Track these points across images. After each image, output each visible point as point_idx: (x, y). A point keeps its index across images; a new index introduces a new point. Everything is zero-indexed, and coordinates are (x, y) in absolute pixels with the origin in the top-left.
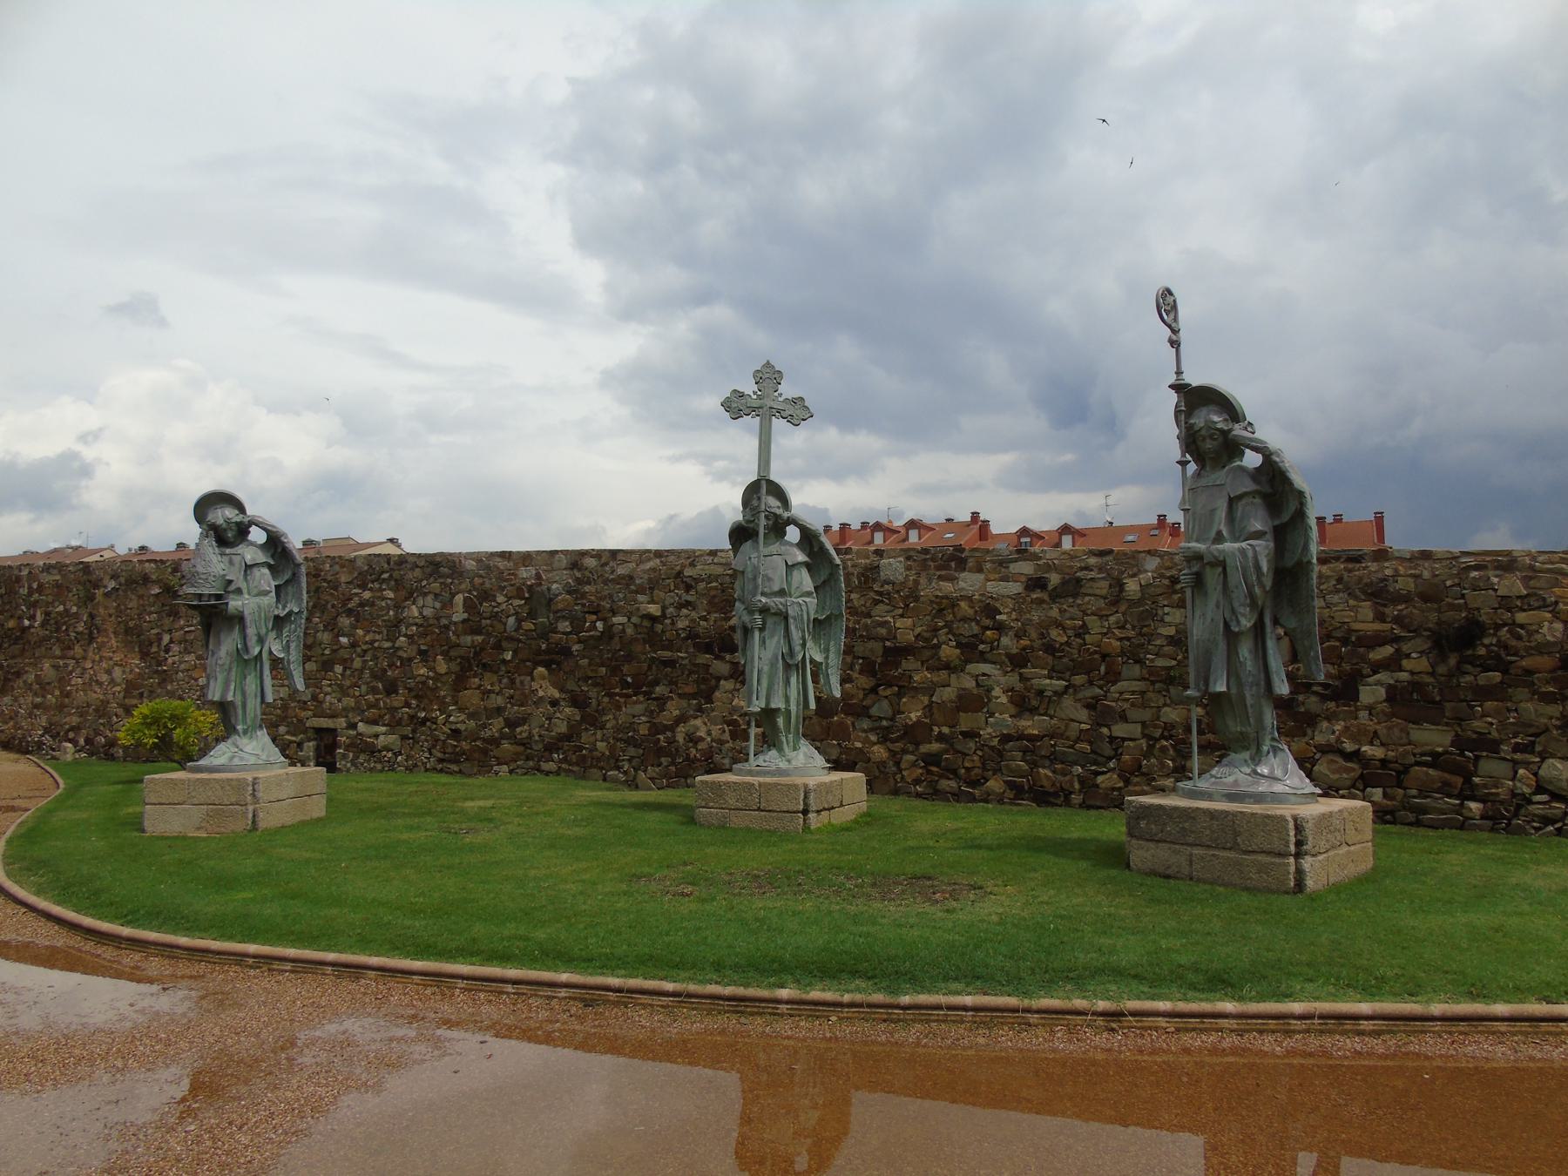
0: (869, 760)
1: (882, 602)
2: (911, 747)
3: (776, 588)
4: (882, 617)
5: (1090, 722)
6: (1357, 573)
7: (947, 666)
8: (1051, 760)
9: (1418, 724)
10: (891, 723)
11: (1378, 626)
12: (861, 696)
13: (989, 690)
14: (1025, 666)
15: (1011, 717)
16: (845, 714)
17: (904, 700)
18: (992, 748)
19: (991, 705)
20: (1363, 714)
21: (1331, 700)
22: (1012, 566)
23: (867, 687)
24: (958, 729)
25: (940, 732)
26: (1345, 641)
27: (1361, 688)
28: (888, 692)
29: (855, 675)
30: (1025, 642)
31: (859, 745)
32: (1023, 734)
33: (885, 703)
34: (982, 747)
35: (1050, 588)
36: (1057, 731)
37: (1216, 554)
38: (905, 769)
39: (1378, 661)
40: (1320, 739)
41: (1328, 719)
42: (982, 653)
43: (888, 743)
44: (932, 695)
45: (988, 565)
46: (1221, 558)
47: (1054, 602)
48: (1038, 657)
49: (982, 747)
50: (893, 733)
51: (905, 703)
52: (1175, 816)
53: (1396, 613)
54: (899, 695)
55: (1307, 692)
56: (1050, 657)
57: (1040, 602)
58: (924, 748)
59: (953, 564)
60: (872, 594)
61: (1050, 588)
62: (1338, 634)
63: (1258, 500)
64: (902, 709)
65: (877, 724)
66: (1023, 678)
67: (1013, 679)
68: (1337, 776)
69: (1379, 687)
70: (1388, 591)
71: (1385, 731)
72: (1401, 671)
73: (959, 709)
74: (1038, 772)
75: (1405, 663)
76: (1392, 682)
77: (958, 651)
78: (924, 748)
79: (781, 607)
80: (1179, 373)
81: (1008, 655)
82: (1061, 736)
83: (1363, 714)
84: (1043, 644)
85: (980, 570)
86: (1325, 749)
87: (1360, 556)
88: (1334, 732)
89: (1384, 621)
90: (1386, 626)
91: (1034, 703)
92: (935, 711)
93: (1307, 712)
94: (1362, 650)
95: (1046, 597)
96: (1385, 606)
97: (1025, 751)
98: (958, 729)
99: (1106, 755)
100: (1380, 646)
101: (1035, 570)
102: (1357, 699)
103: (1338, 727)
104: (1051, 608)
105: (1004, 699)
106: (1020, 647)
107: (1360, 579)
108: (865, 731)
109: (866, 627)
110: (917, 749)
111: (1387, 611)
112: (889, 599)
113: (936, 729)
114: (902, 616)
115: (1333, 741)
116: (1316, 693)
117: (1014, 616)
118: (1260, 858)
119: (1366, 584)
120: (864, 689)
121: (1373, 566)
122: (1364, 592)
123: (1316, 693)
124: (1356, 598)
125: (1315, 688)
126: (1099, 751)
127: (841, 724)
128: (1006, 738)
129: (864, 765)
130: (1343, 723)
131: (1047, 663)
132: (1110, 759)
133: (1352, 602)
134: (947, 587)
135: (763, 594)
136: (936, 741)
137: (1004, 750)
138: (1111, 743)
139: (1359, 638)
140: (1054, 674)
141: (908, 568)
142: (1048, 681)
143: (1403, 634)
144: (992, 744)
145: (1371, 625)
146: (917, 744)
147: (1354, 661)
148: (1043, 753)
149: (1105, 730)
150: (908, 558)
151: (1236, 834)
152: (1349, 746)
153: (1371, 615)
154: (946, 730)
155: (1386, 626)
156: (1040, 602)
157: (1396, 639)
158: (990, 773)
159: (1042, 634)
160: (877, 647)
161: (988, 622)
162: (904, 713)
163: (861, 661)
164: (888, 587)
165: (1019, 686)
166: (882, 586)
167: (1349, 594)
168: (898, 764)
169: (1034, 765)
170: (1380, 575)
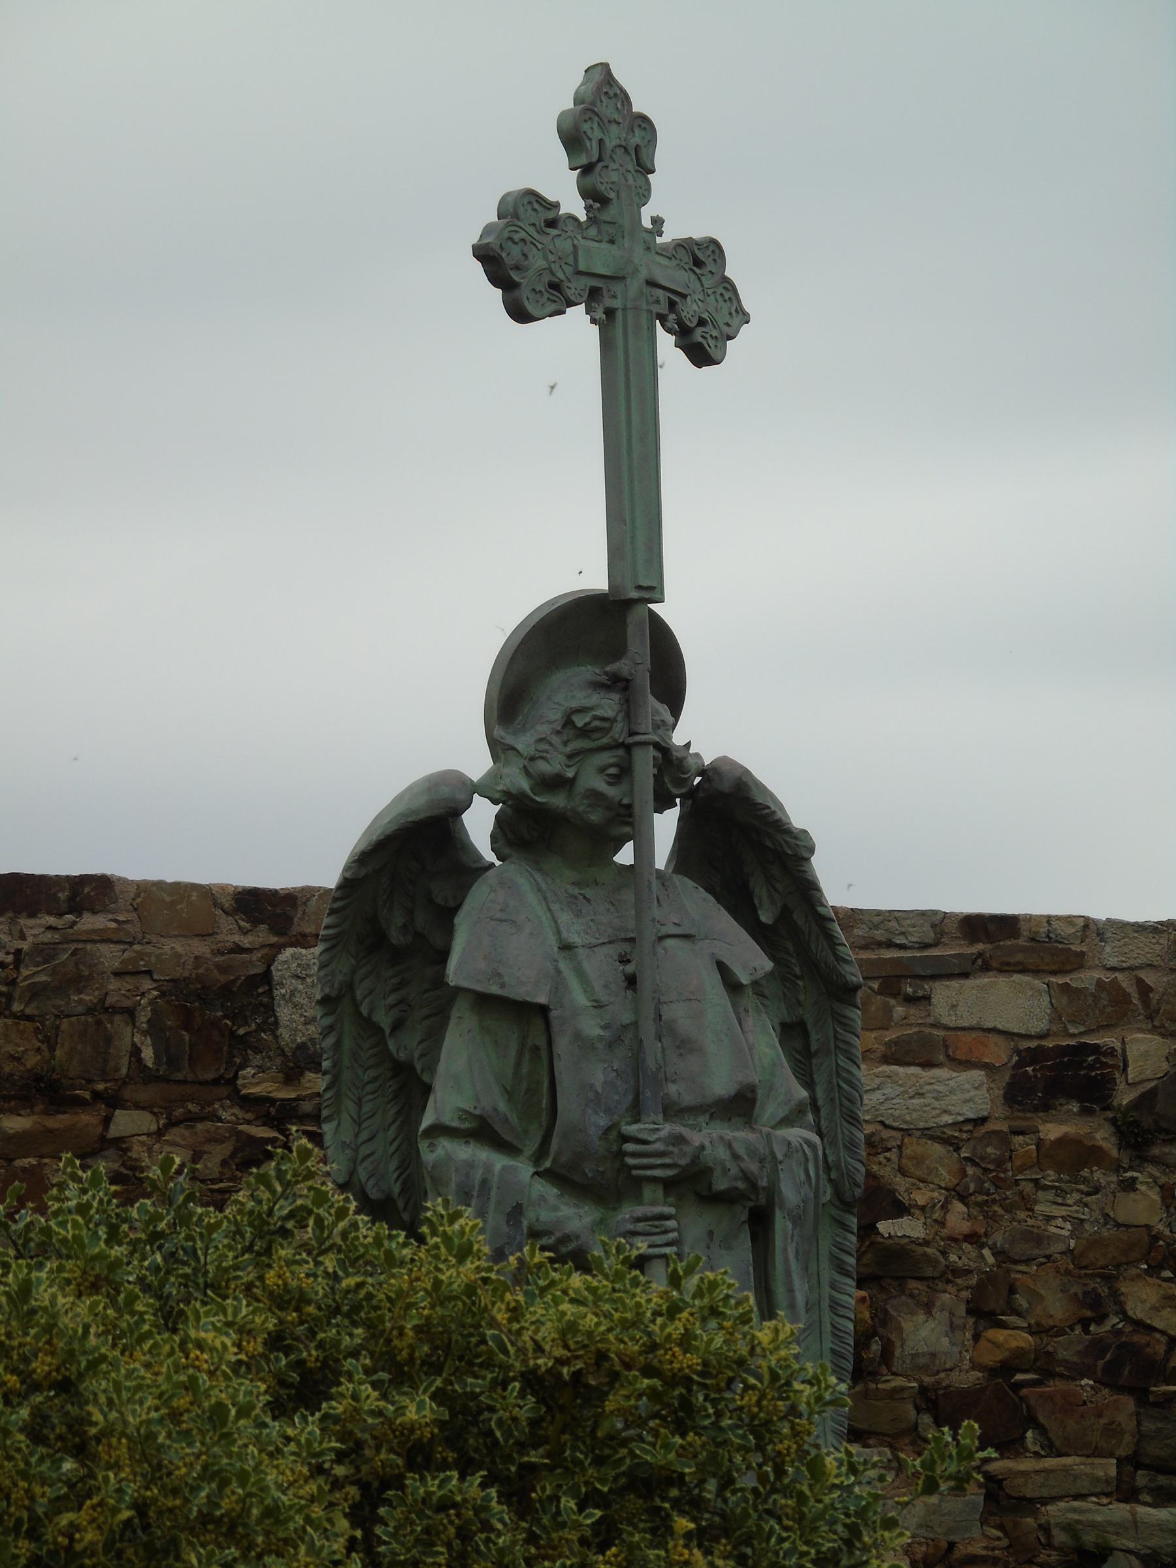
3: (721, 1084)
35: (1125, 1097)
56: (1129, 1404)
61: (1125, 1097)
79: (753, 1167)
84: (1097, 1347)
101: (1056, 1015)
104: (1129, 1186)
131: (1113, 1430)
135: (671, 1111)
140: (1142, 1478)
142: (1120, 1511)
166: (291, 1076)
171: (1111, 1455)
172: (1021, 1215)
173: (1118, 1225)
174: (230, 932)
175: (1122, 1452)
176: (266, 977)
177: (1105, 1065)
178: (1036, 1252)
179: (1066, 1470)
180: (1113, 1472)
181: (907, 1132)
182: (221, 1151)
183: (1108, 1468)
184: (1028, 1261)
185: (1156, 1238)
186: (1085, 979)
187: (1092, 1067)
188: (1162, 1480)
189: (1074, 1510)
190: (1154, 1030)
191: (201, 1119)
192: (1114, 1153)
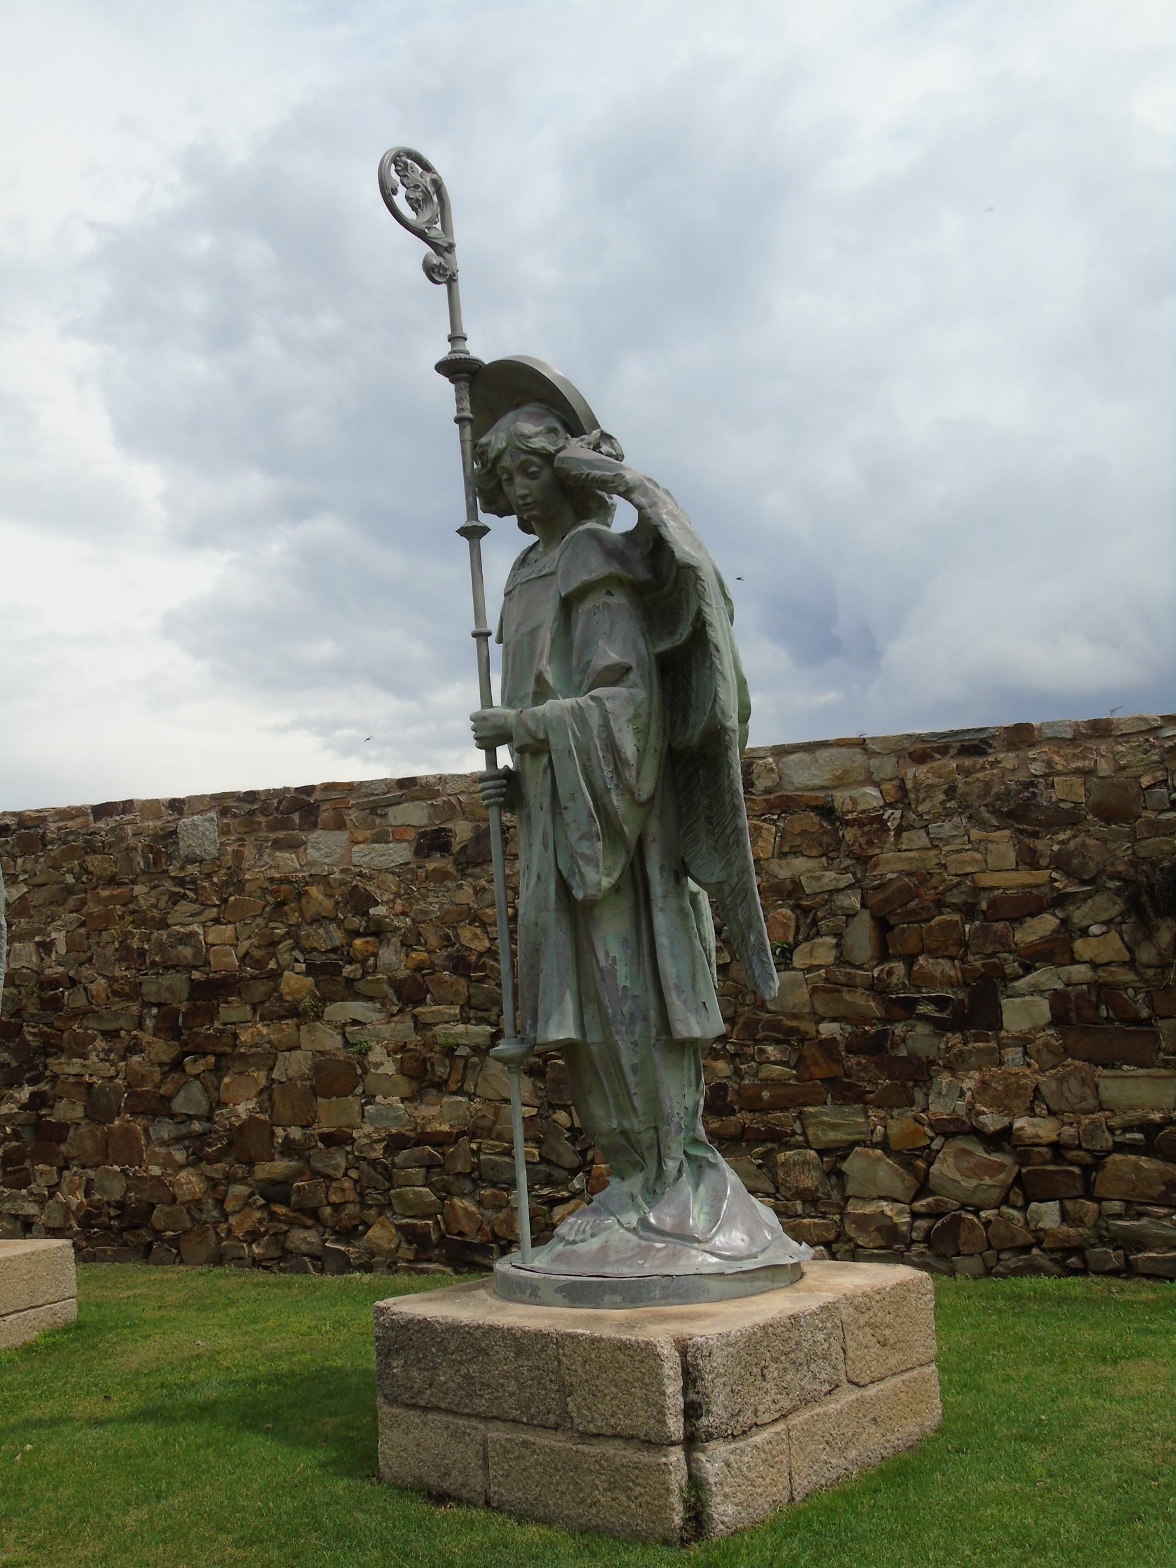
0: (174, 1200)
1: (184, 897)
2: (241, 1170)
4: (182, 925)
5: (536, 1102)
6: (980, 775)
7: (294, 1012)
8: (474, 1181)
9: (1113, 1067)
10: (206, 1125)
11: (1026, 877)
12: (157, 1077)
13: (364, 1053)
14: (421, 1002)
15: (403, 1100)
16: (132, 1114)
17: (226, 1080)
18: (374, 1163)
19: (369, 1079)
20: (1013, 1054)
21: (953, 1030)
22: (392, 812)
23: (165, 1058)
24: (316, 1130)
25: (286, 1138)
26: (969, 911)
27: (1004, 1001)
28: (200, 1066)
29: (146, 1037)
30: (419, 955)
31: (156, 1171)
32: (423, 1133)
33: (196, 1088)
34: (356, 1162)
35: (456, 848)
36: (482, 1123)
37: (531, 725)
38: (234, 1213)
39: (1032, 945)
40: (940, 1108)
41: (950, 1068)
42: (350, 981)
43: (204, 1166)
44: (271, 1069)
45: (354, 814)
46: (541, 736)
47: (464, 875)
48: (441, 983)
49: (356, 1162)
50: (210, 1145)
51: (227, 1085)
52: (452, 1347)
53: (1056, 848)
54: (218, 1070)
55: (909, 1018)
56: (463, 982)
57: (441, 876)
58: (263, 1171)
59: (296, 817)
60: (168, 885)
61: (456, 848)
62: (955, 898)
63: (619, 599)
64: (224, 1096)
65: (183, 1129)
66: (420, 1026)
67: (403, 1029)
68: (974, 1182)
69: (1037, 998)
70: (1038, 806)
71: (1054, 1085)
72: (1074, 962)
73: (315, 1092)
74: (452, 1206)
75: (1079, 945)
76: (1059, 986)
77: (310, 981)
78: (263, 1171)
80: (456, 337)
81: (392, 982)
82: (489, 1132)
83: (1013, 1054)
84: (450, 957)
85: (340, 825)
86: (951, 1129)
87: (983, 741)
88: (962, 1094)
89: (1035, 866)
90: (1040, 876)
91: (441, 1071)
92: (277, 1097)
93: (912, 1058)
94: (999, 926)
95: (451, 868)
96: (1035, 835)
97: (430, 1166)
98: (316, 1130)
99: (567, 1165)
100: (1033, 915)
101: (430, 817)
102: (997, 1024)
103: (969, 1083)
104: (460, 887)
105: (389, 1068)
106: (411, 965)
107: (987, 785)
108: (164, 1143)
109: (160, 946)
110: (251, 1173)
111: (1039, 845)
112: (195, 891)
113: (279, 1131)
114: (217, 921)
115: (962, 1112)
116: (924, 1018)
117: (399, 907)
118: (612, 1449)
119: (998, 797)
120: (161, 1064)
121: (1009, 760)
122: (996, 812)
123: (924, 1018)
124: (982, 824)
125: (922, 1009)
126: (554, 1158)
127: (126, 1131)
128: (396, 1143)
129: (167, 1209)
130: (976, 1075)
131: (457, 993)
132: (574, 1172)
133: (975, 834)
134: (288, 861)
136: (283, 1154)
137: (394, 1164)
138: (573, 1140)
139: (993, 904)
140: (472, 1014)
141: (224, 831)
142: (461, 1028)
143: (1071, 890)
144: (374, 1155)
145: (1014, 874)
146: (251, 1164)
147: (989, 949)
148: (459, 1168)
149: (562, 1117)
150: (224, 812)
151: (565, 1391)
152: (991, 1121)
153: (1012, 856)
154: (296, 1133)
155: (1040, 876)
156: (441, 876)
157: (1061, 900)
158: (373, 1212)
159: (447, 938)
160: (176, 981)
161: (356, 922)
162: (225, 1105)
163: (155, 1011)
164: (193, 869)
165: (414, 1040)
166: (183, 868)
167: (970, 818)
168: (220, 1202)
169: (445, 1192)
170: (1022, 777)
171: (457, 1004)
172: (421, 902)
173: (457, 905)
174: (168, 815)
175: (461, 1003)
176: (175, 832)
177: (448, 836)
178: (426, 918)
179: (439, 1011)
180: (458, 1011)
181: (380, 871)
182: (165, 898)
183: (456, 1010)
184: (424, 922)
185: (470, 909)
186: (438, 802)
187: (443, 838)
188: (480, 1014)
189: (444, 1028)
190: (466, 819)
191: (159, 886)
192: (455, 873)
